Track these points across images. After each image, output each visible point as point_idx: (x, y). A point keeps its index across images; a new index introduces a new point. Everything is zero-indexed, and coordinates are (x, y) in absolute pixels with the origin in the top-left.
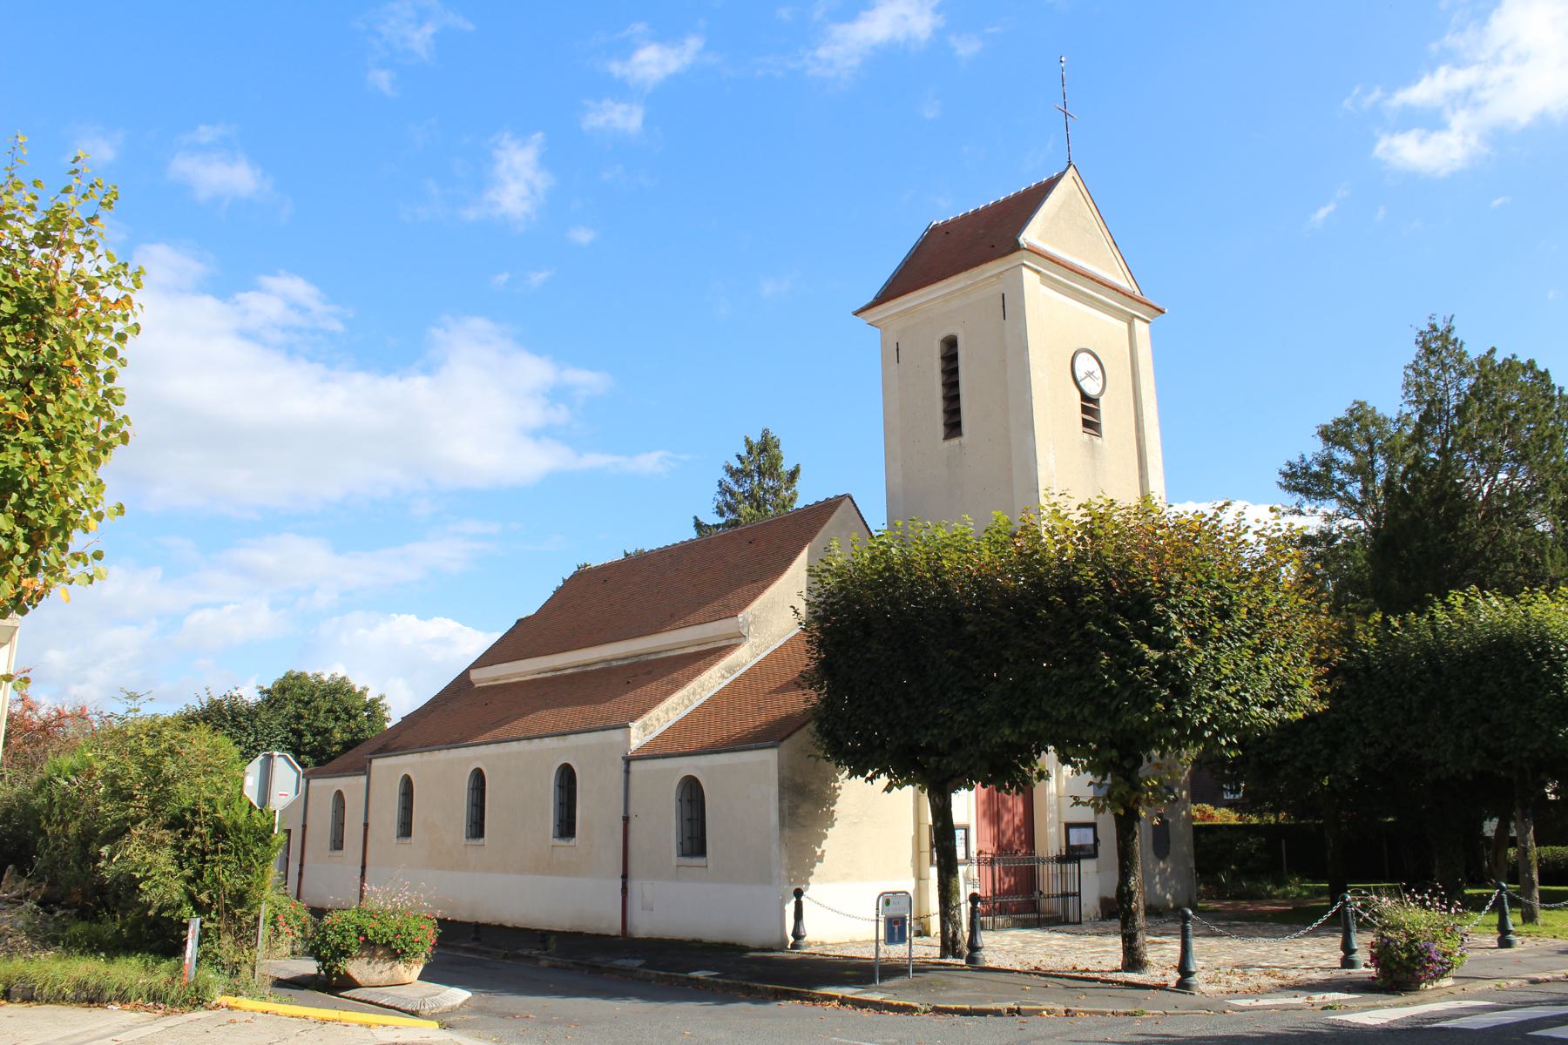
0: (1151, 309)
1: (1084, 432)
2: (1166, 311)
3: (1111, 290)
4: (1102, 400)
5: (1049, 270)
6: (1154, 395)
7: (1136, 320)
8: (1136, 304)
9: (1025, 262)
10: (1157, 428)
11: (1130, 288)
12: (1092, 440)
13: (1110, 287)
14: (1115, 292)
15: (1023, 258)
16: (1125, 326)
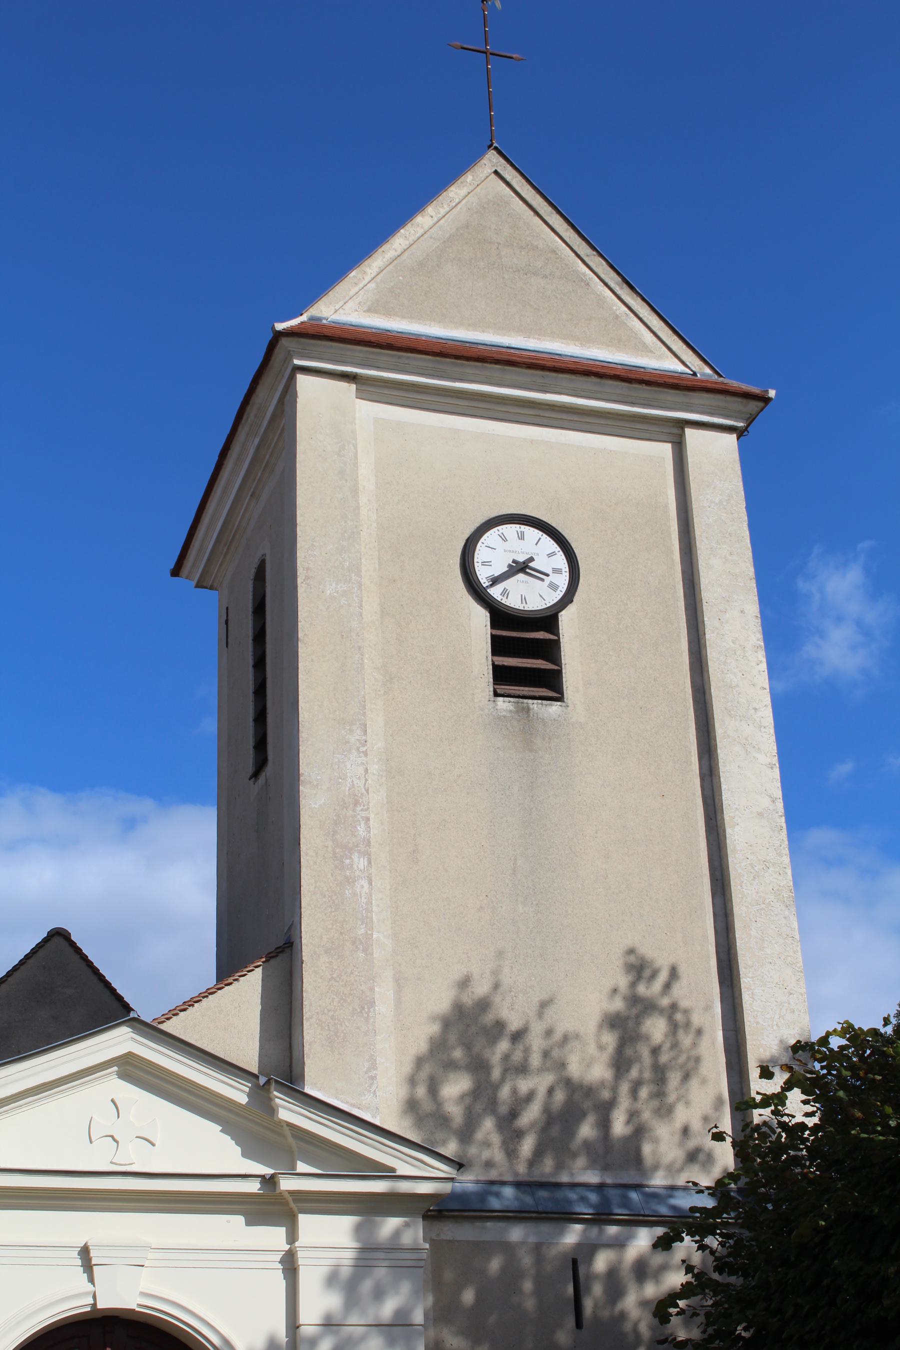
0: (721, 397)
1: (496, 694)
2: (772, 393)
3: (644, 387)
4: (565, 617)
5: (378, 368)
6: (753, 584)
7: (689, 432)
8: (471, 368)
9: (297, 362)
10: (761, 656)
11: (680, 368)
12: (528, 710)
13: (497, 362)
14: (594, 379)
15: (289, 356)
16: (666, 450)
